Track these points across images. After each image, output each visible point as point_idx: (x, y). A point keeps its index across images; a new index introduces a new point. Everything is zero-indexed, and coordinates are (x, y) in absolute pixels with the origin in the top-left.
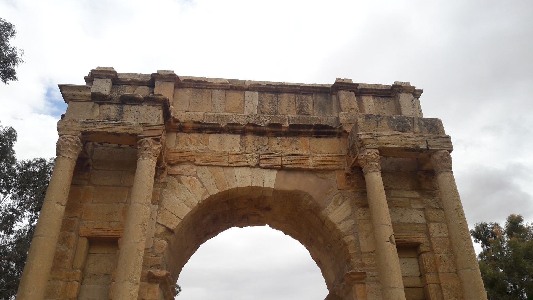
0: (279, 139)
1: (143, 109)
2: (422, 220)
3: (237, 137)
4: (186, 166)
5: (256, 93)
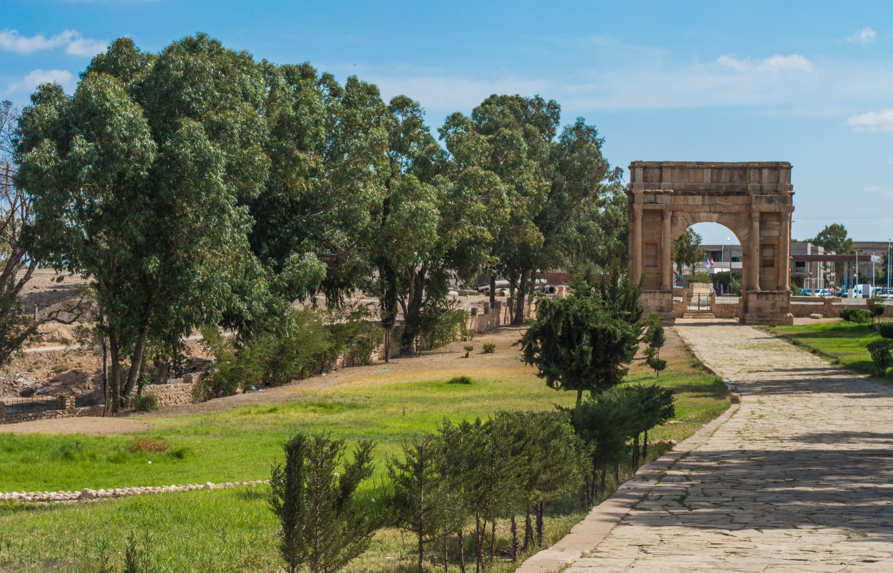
0: (720, 198)
1: (663, 196)
2: (778, 235)
3: (701, 197)
4: (680, 212)
5: (710, 170)
